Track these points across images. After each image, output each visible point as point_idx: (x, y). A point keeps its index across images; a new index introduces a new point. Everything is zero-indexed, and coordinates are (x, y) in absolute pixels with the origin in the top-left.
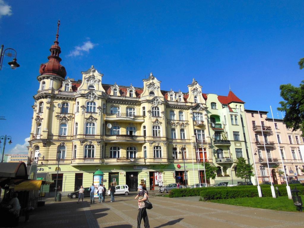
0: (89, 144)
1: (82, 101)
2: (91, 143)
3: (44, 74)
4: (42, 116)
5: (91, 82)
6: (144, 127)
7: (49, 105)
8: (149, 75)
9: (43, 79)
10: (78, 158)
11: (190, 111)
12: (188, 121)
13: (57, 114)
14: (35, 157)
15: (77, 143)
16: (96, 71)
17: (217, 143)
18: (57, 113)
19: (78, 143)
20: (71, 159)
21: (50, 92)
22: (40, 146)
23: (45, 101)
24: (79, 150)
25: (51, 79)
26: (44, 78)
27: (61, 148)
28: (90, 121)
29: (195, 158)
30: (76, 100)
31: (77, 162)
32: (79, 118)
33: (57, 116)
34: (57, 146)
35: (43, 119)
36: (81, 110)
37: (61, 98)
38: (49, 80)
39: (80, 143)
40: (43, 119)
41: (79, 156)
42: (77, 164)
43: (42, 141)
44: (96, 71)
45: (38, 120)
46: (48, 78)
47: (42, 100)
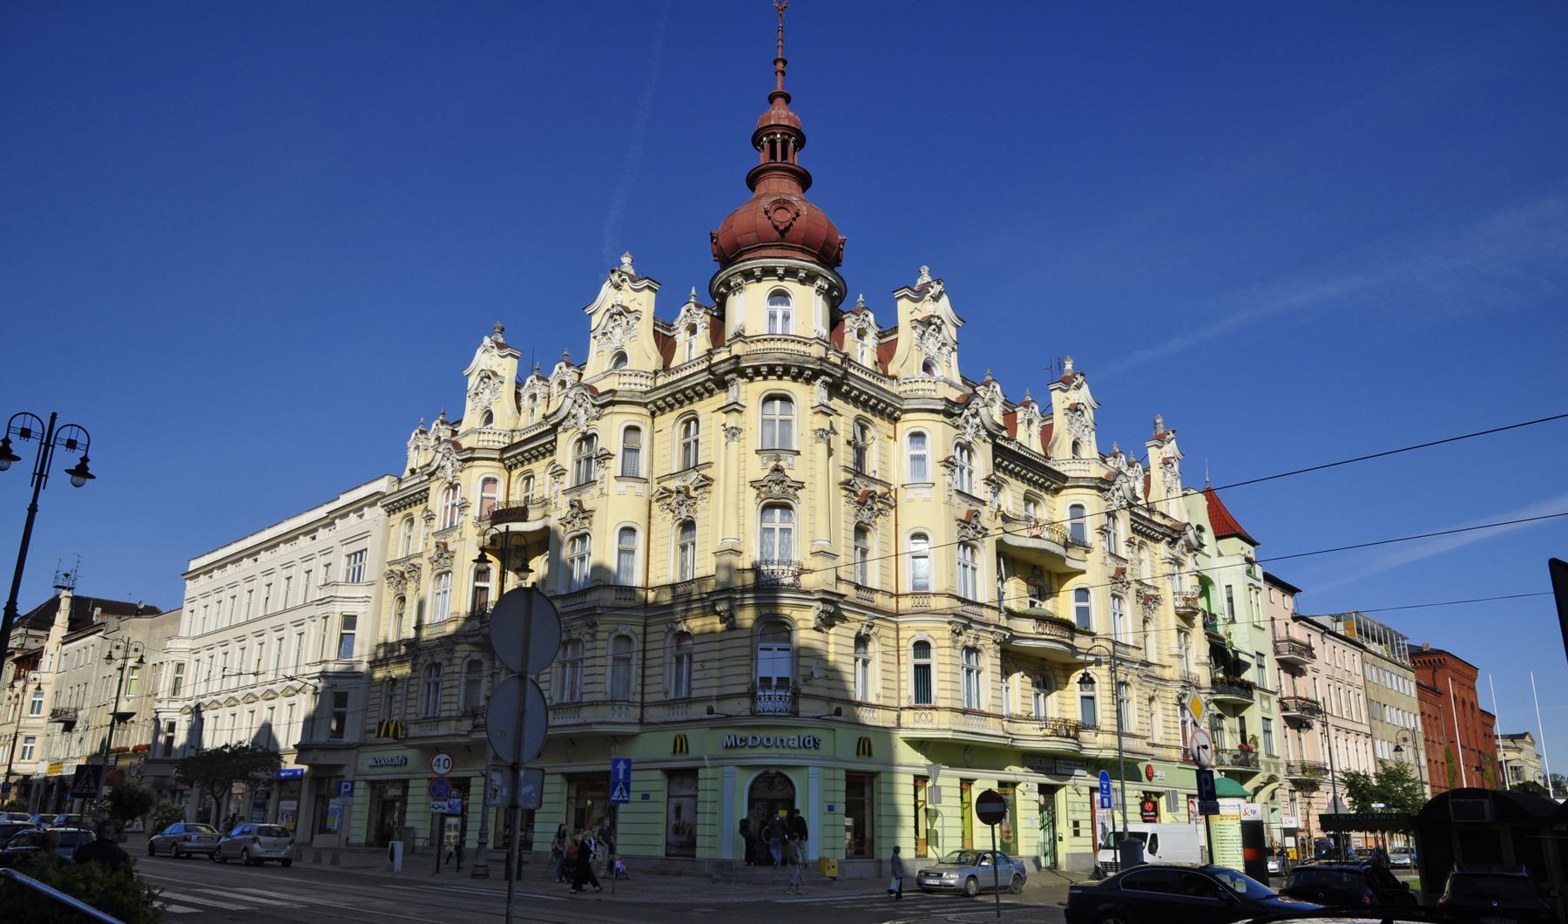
0: (970, 644)
1: (940, 436)
2: (977, 639)
3: (764, 253)
4: (795, 470)
5: (931, 345)
6: (1082, 593)
7: (822, 422)
8: (1061, 366)
9: (781, 279)
10: (948, 703)
11: (1162, 549)
12: (1156, 588)
13: (844, 476)
14: (762, 673)
15: (933, 633)
16: (945, 299)
17: (1219, 693)
18: (846, 469)
19: (939, 634)
20: (895, 703)
21: (816, 351)
22: (801, 624)
23: (807, 396)
24: (948, 669)
25: (820, 290)
26: (791, 273)
27: (861, 641)
28: (969, 531)
29: (1181, 744)
30: (897, 420)
31: (939, 725)
32: (925, 508)
33: (847, 483)
34: (853, 634)
35: (800, 486)
36: (934, 471)
37: (856, 401)
38: (810, 290)
39: (947, 634)
40: (800, 486)
41: (948, 694)
42: (949, 735)
43: (823, 601)
44: (945, 299)
45: (777, 489)
46: (810, 279)
47: (786, 385)
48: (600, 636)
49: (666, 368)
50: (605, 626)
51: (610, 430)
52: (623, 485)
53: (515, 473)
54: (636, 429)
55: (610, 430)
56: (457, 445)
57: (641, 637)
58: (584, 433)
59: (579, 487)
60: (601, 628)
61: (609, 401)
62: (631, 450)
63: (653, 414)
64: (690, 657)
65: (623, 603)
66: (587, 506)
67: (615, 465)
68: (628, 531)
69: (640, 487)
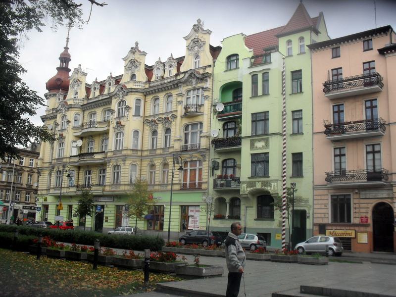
48: (126, 164)
49: (149, 81)
50: (128, 162)
51: (131, 100)
52: (135, 118)
53: (87, 113)
54: (139, 100)
55: (131, 100)
56: (66, 103)
57: (140, 166)
58: (121, 100)
59: (119, 117)
60: (127, 162)
61: (132, 91)
62: (138, 108)
63: (145, 96)
64: (155, 172)
65: (134, 155)
66: (122, 123)
67: (133, 111)
68: (136, 132)
69: (139, 119)
